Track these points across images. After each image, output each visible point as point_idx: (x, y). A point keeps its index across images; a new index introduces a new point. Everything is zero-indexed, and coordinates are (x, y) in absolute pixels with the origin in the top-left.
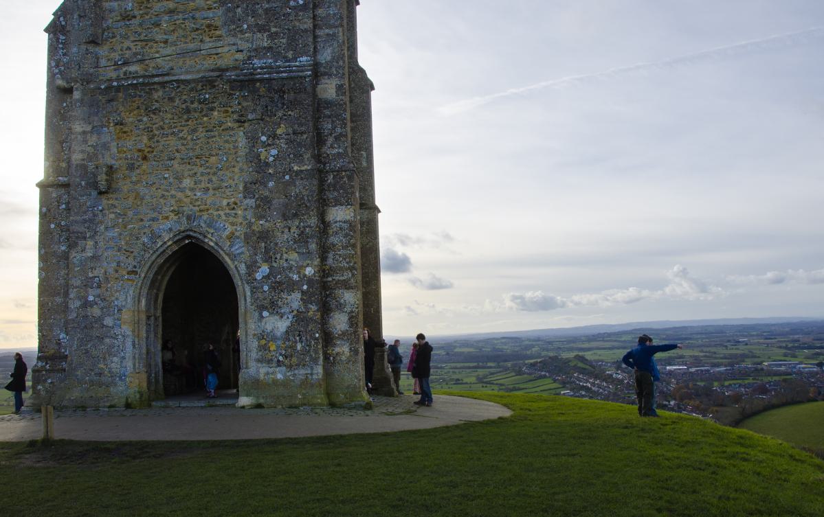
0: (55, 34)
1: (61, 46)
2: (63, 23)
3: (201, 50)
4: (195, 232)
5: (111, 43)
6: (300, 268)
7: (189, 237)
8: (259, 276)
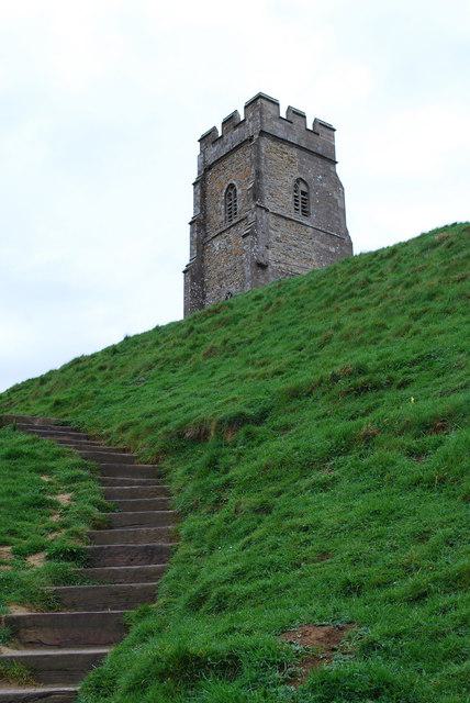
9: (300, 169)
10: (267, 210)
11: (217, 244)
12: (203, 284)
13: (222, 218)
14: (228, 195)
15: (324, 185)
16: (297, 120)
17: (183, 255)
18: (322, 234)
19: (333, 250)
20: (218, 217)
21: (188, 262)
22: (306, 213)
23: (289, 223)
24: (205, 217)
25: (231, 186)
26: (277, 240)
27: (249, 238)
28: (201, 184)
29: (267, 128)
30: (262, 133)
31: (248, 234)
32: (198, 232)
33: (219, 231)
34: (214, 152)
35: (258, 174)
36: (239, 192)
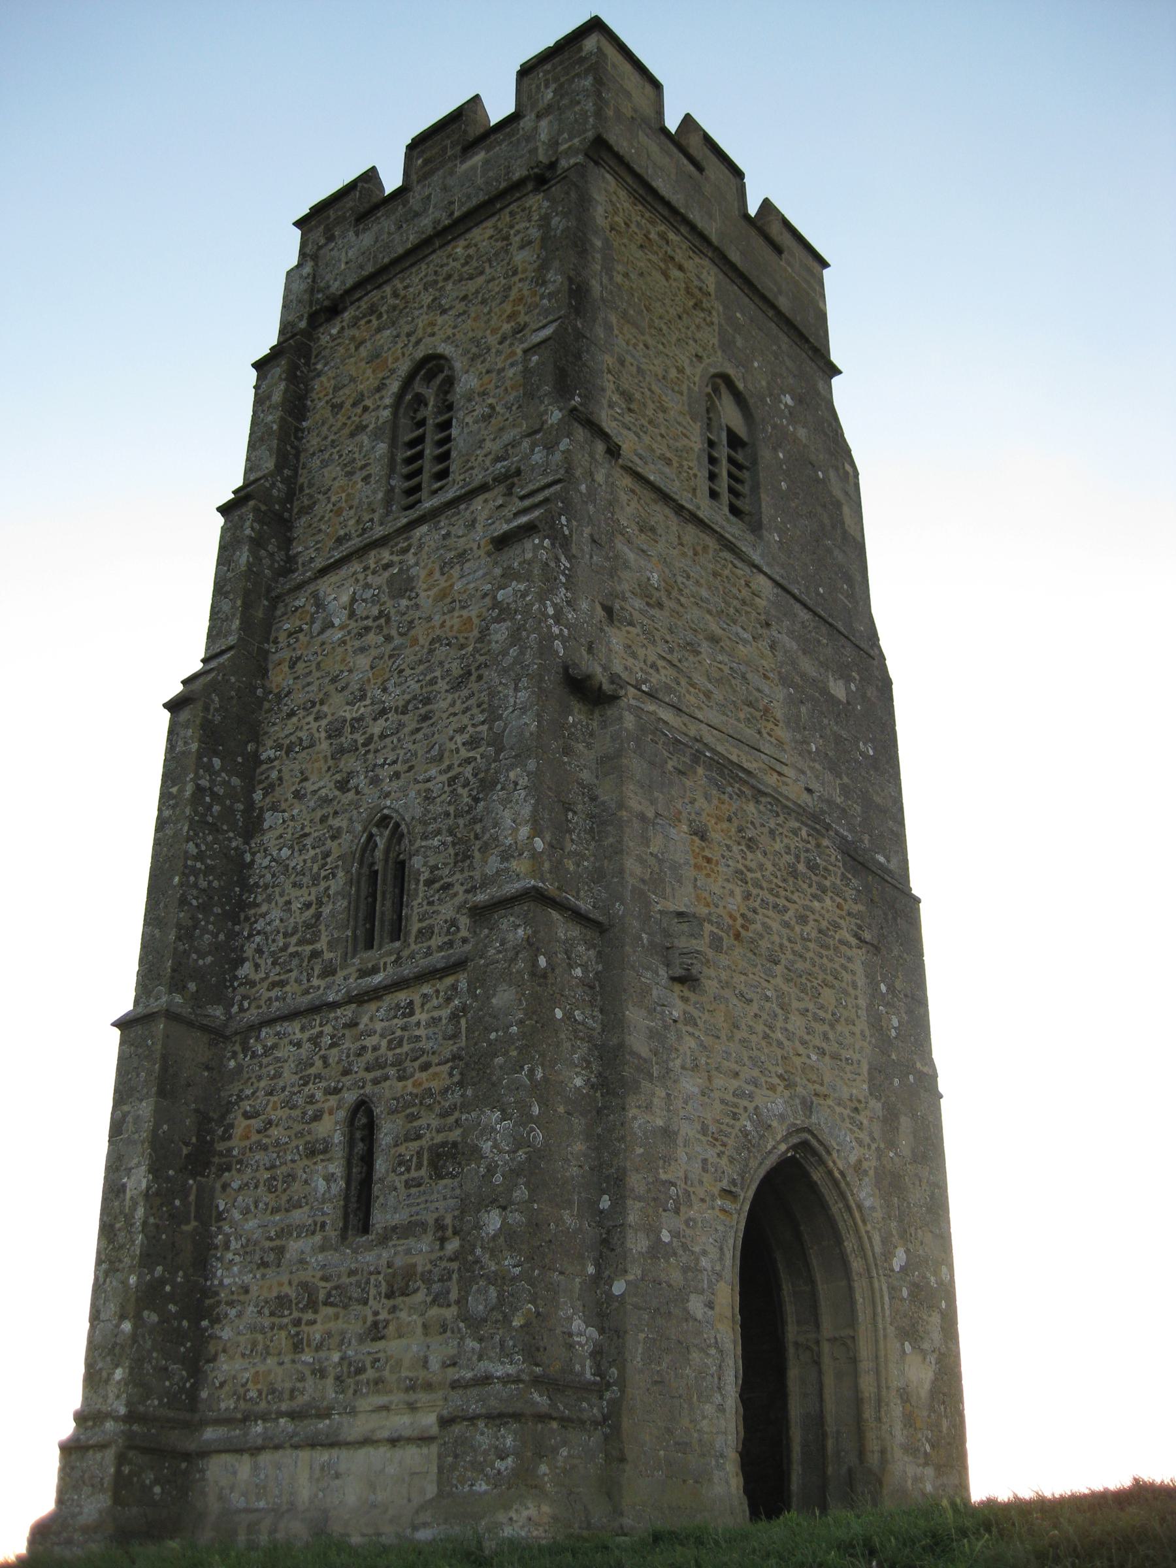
0: (553, 544)
2: (567, 532)
5: (628, 632)
9: (726, 344)
10: (613, 451)
11: (338, 593)
12: (250, 769)
14: (408, 402)
17: (176, 638)
18: (804, 615)
19: (838, 690)
20: (351, 482)
23: (691, 533)
24: (290, 496)
25: (432, 367)
26: (644, 591)
27: (536, 549)
28: (290, 377)
29: (618, 138)
30: (600, 150)
31: (530, 529)
32: (257, 543)
33: (356, 542)
34: (353, 251)
35: (578, 295)
36: (467, 382)
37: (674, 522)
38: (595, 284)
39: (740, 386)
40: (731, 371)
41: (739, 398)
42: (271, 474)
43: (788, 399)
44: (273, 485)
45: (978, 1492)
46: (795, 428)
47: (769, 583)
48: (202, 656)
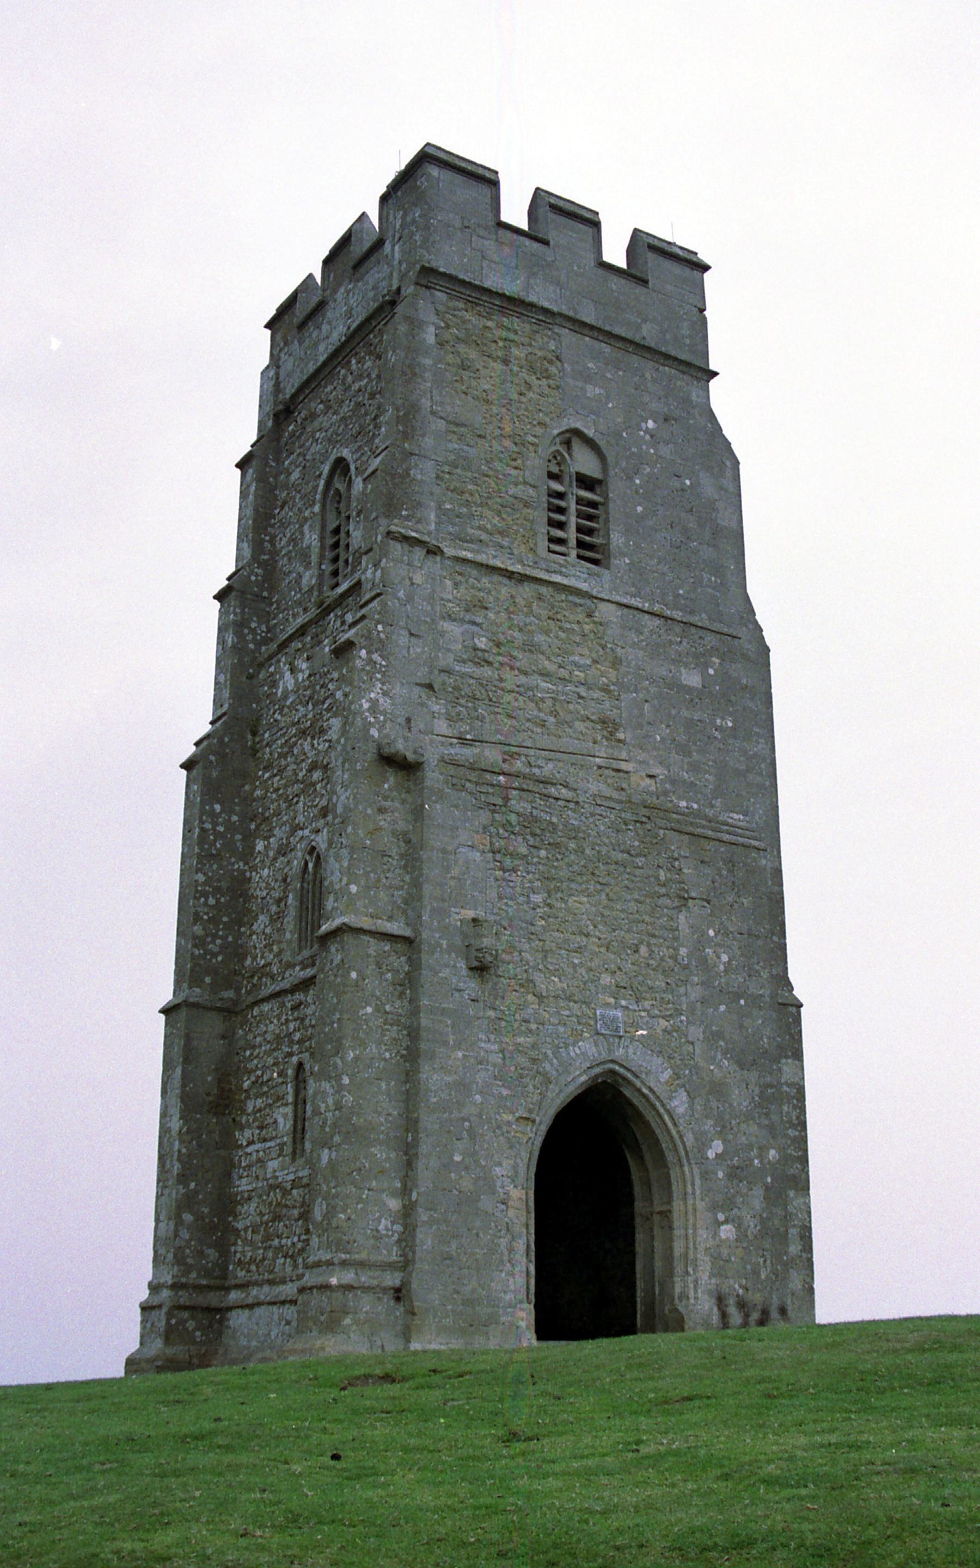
1: (379, 676)
3: (594, 756)
4: (621, 1066)
6: (763, 1150)
7: (612, 1072)
8: (711, 1154)
13: (309, 578)
15: (666, 451)
16: (561, 233)
19: (692, 679)
21: (205, 728)
22: (592, 552)
30: (429, 276)
37: (505, 589)
38: (426, 403)
39: (590, 433)
40: (579, 425)
41: (590, 443)
42: (249, 565)
43: (651, 424)
44: (252, 573)
45: (817, 1322)
46: (656, 450)
47: (612, 607)
48: (211, 719)
